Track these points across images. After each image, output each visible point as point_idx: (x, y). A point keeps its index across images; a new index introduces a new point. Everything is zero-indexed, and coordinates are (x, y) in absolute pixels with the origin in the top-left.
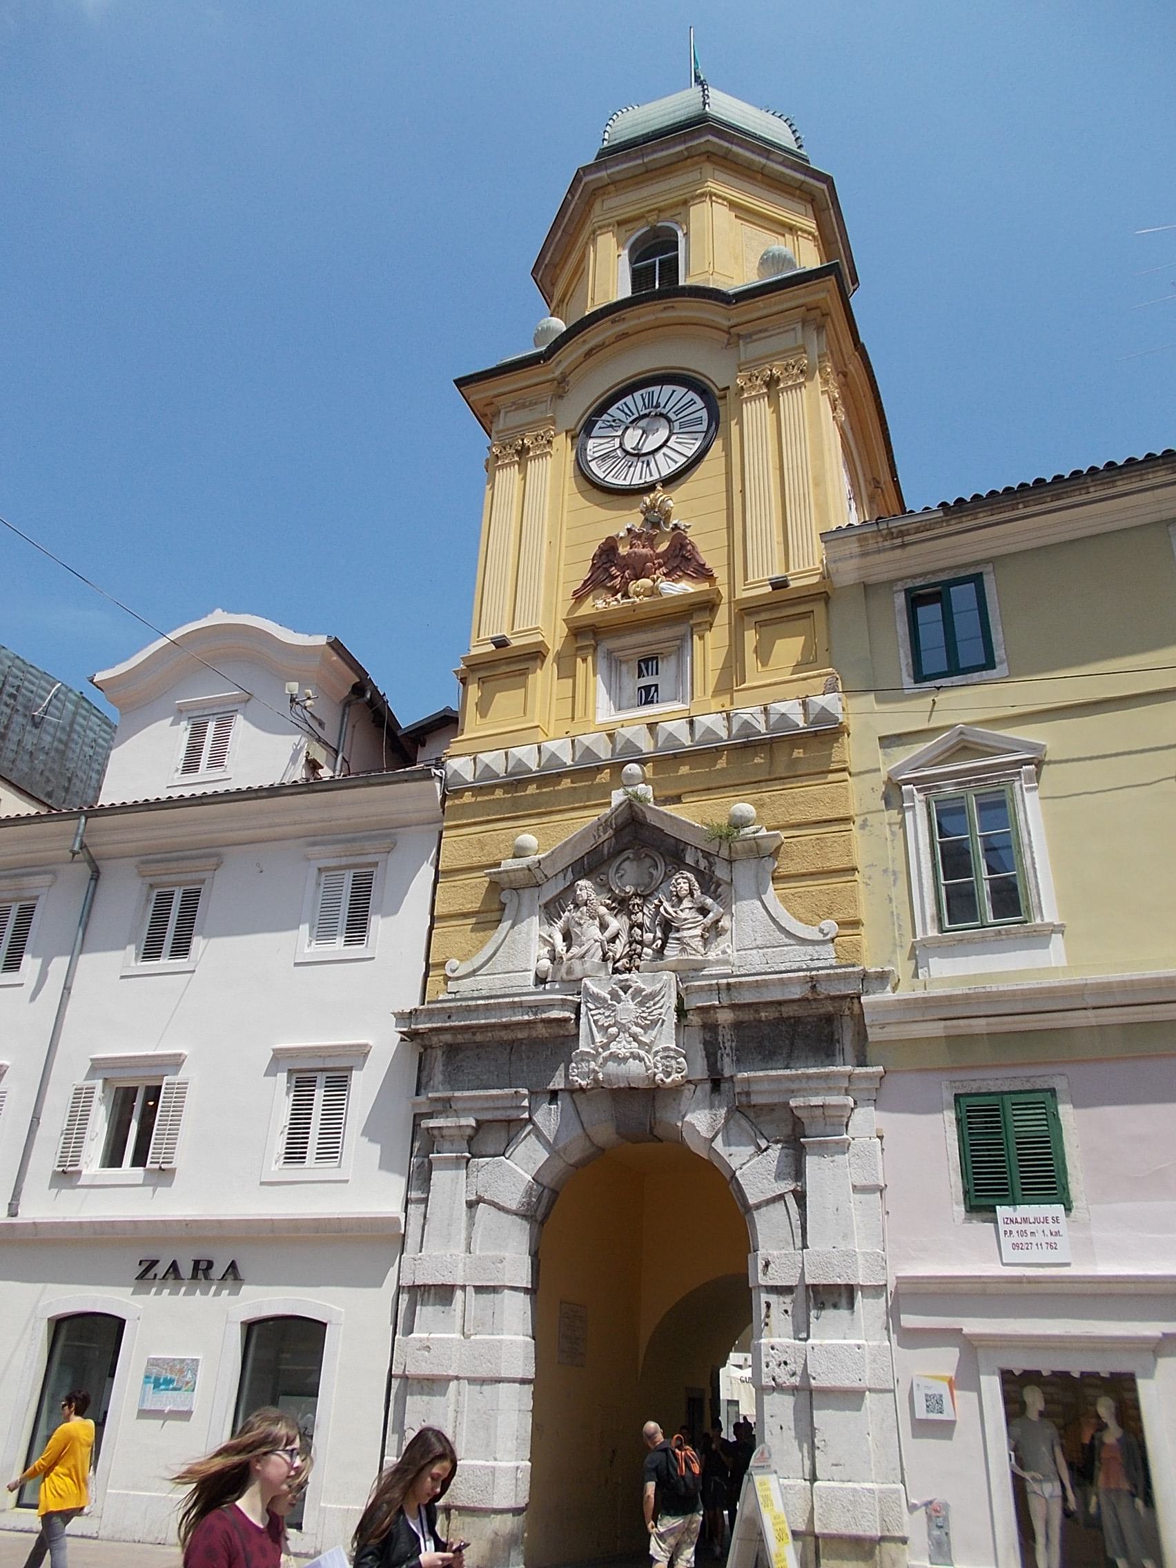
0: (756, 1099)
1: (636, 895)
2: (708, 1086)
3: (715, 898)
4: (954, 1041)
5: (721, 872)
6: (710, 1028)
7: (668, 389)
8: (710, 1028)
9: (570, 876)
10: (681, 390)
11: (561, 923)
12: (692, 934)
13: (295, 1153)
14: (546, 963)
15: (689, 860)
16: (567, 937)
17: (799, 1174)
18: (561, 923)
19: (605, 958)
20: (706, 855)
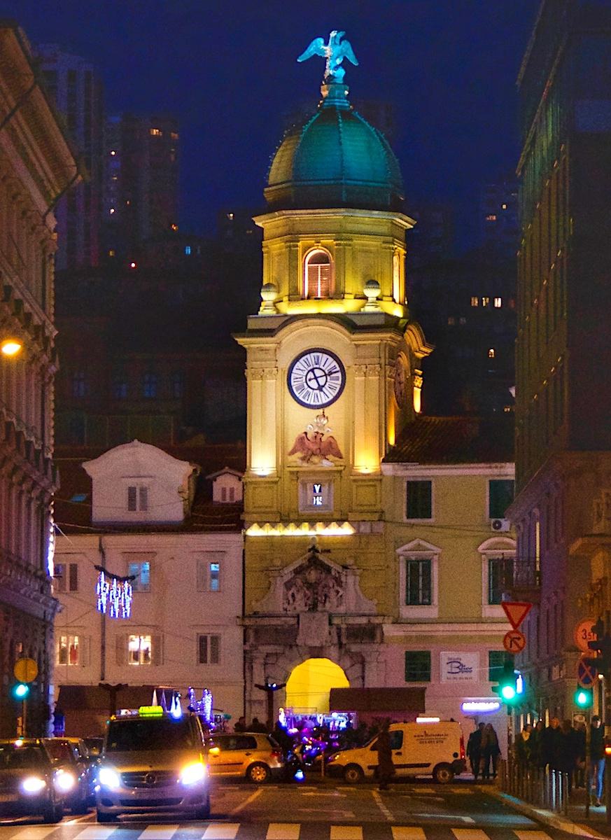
0: (353, 651)
1: (316, 583)
2: (338, 646)
3: (341, 586)
4: (406, 637)
5: (343, 579)
6: (339, 629)
7: (325, 356)
8: (339, 629)
9: (293, 574)
10: (331, 359)
11: (290, 593)
12: (335, 600)
13: (203, 660)
14: (286, 606)
15: (333, 574)
16: (293, 595)
17: (363, 672)
18: (290, 593)
19: (306, 605)
20: (339, 573)
